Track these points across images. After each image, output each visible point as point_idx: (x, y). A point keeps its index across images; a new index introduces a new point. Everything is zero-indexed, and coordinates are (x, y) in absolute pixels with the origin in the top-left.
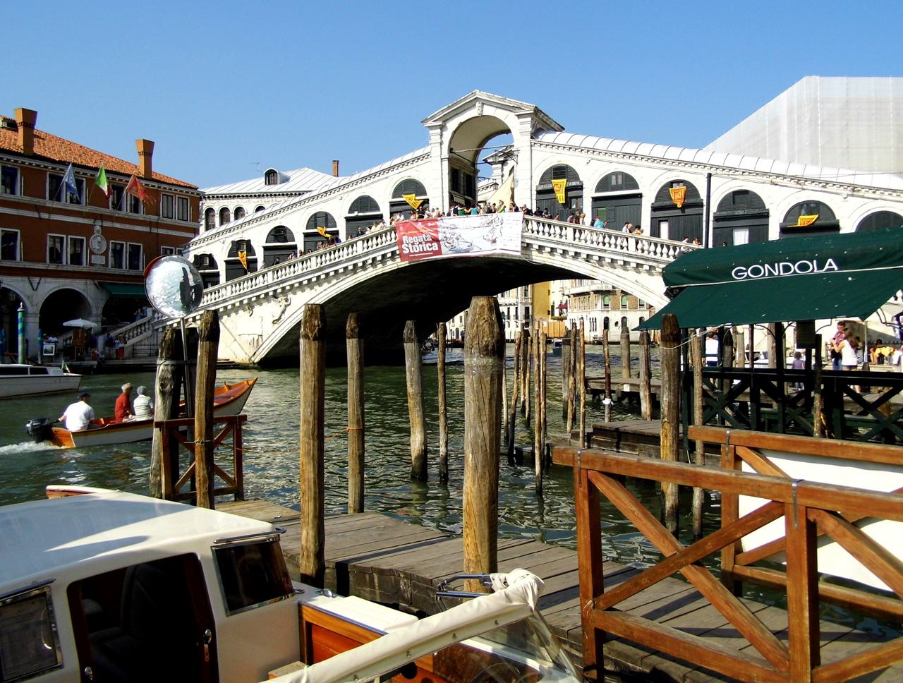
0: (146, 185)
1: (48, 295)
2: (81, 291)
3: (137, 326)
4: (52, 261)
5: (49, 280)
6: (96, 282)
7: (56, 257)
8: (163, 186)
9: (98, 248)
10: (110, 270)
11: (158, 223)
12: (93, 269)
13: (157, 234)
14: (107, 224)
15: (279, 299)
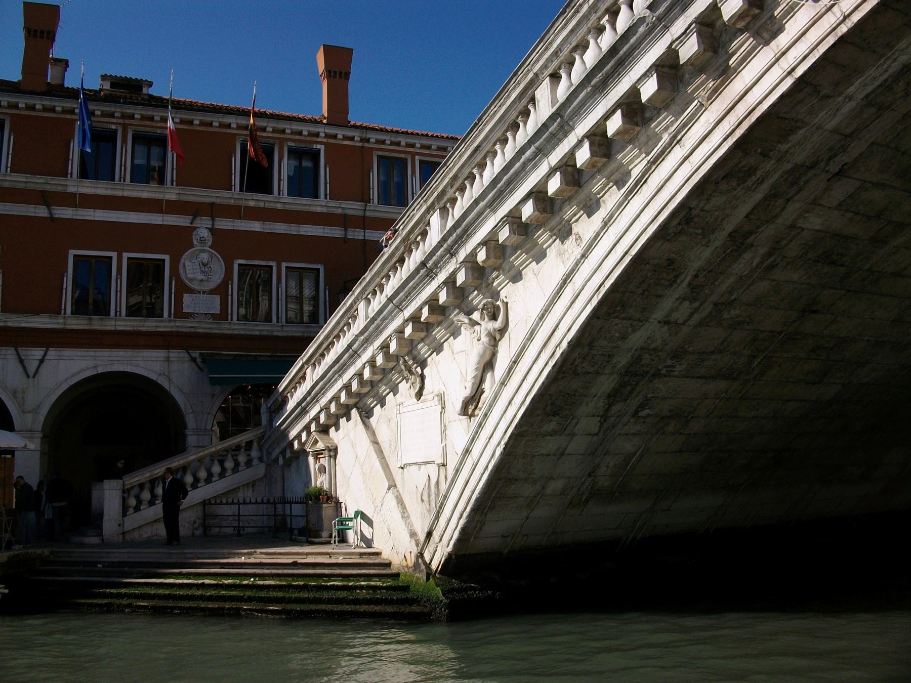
0: (327, 136)
1: (65, 387)
2: (153, 377)
3: (227, 450)
4: (80, 307)
5: (67, 352)
6: (194, 355)
7: (92, 302)
8: (373, 137)
9: (200, 277)
10: (234, 326)
11: (364, 217)
12: (184, 326)
13: (364, 241)
14: (224, 224)
15: (476, 316)
